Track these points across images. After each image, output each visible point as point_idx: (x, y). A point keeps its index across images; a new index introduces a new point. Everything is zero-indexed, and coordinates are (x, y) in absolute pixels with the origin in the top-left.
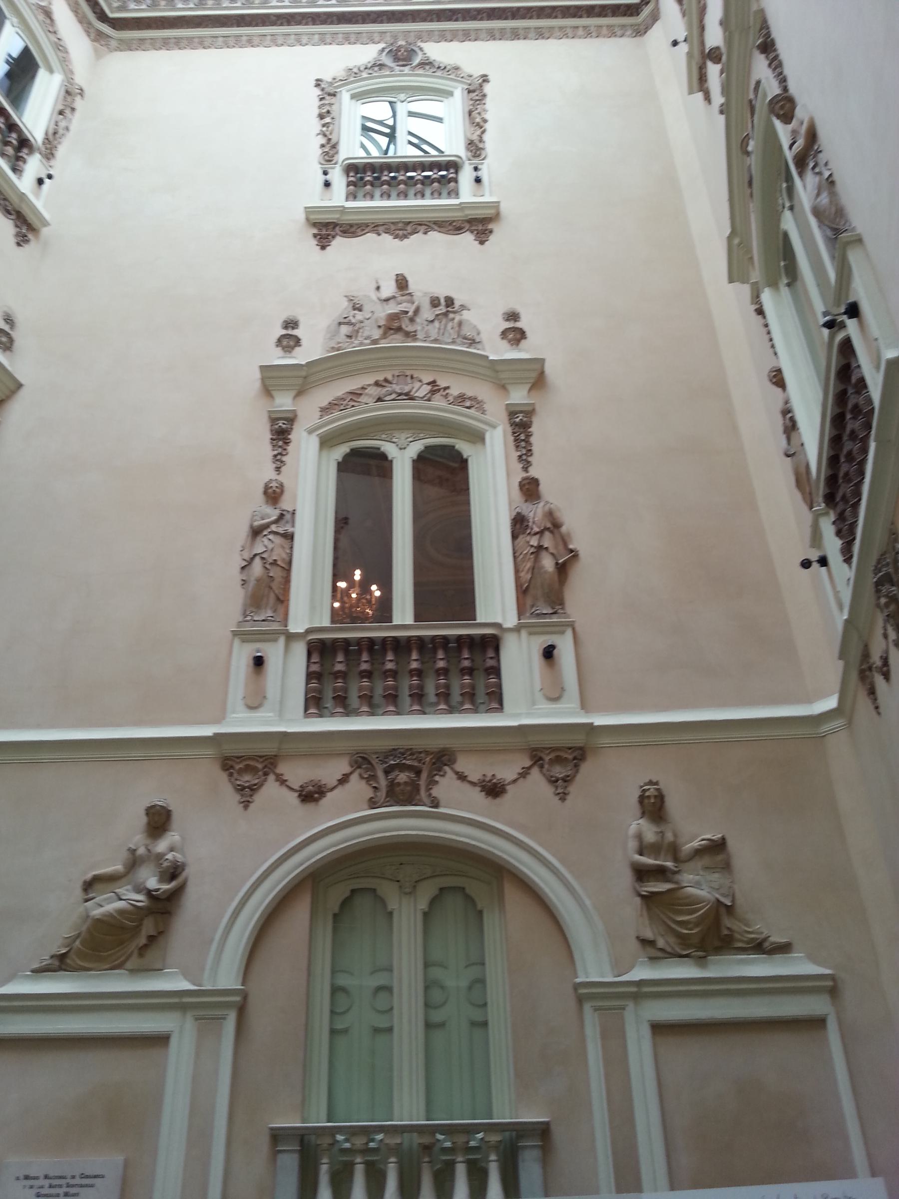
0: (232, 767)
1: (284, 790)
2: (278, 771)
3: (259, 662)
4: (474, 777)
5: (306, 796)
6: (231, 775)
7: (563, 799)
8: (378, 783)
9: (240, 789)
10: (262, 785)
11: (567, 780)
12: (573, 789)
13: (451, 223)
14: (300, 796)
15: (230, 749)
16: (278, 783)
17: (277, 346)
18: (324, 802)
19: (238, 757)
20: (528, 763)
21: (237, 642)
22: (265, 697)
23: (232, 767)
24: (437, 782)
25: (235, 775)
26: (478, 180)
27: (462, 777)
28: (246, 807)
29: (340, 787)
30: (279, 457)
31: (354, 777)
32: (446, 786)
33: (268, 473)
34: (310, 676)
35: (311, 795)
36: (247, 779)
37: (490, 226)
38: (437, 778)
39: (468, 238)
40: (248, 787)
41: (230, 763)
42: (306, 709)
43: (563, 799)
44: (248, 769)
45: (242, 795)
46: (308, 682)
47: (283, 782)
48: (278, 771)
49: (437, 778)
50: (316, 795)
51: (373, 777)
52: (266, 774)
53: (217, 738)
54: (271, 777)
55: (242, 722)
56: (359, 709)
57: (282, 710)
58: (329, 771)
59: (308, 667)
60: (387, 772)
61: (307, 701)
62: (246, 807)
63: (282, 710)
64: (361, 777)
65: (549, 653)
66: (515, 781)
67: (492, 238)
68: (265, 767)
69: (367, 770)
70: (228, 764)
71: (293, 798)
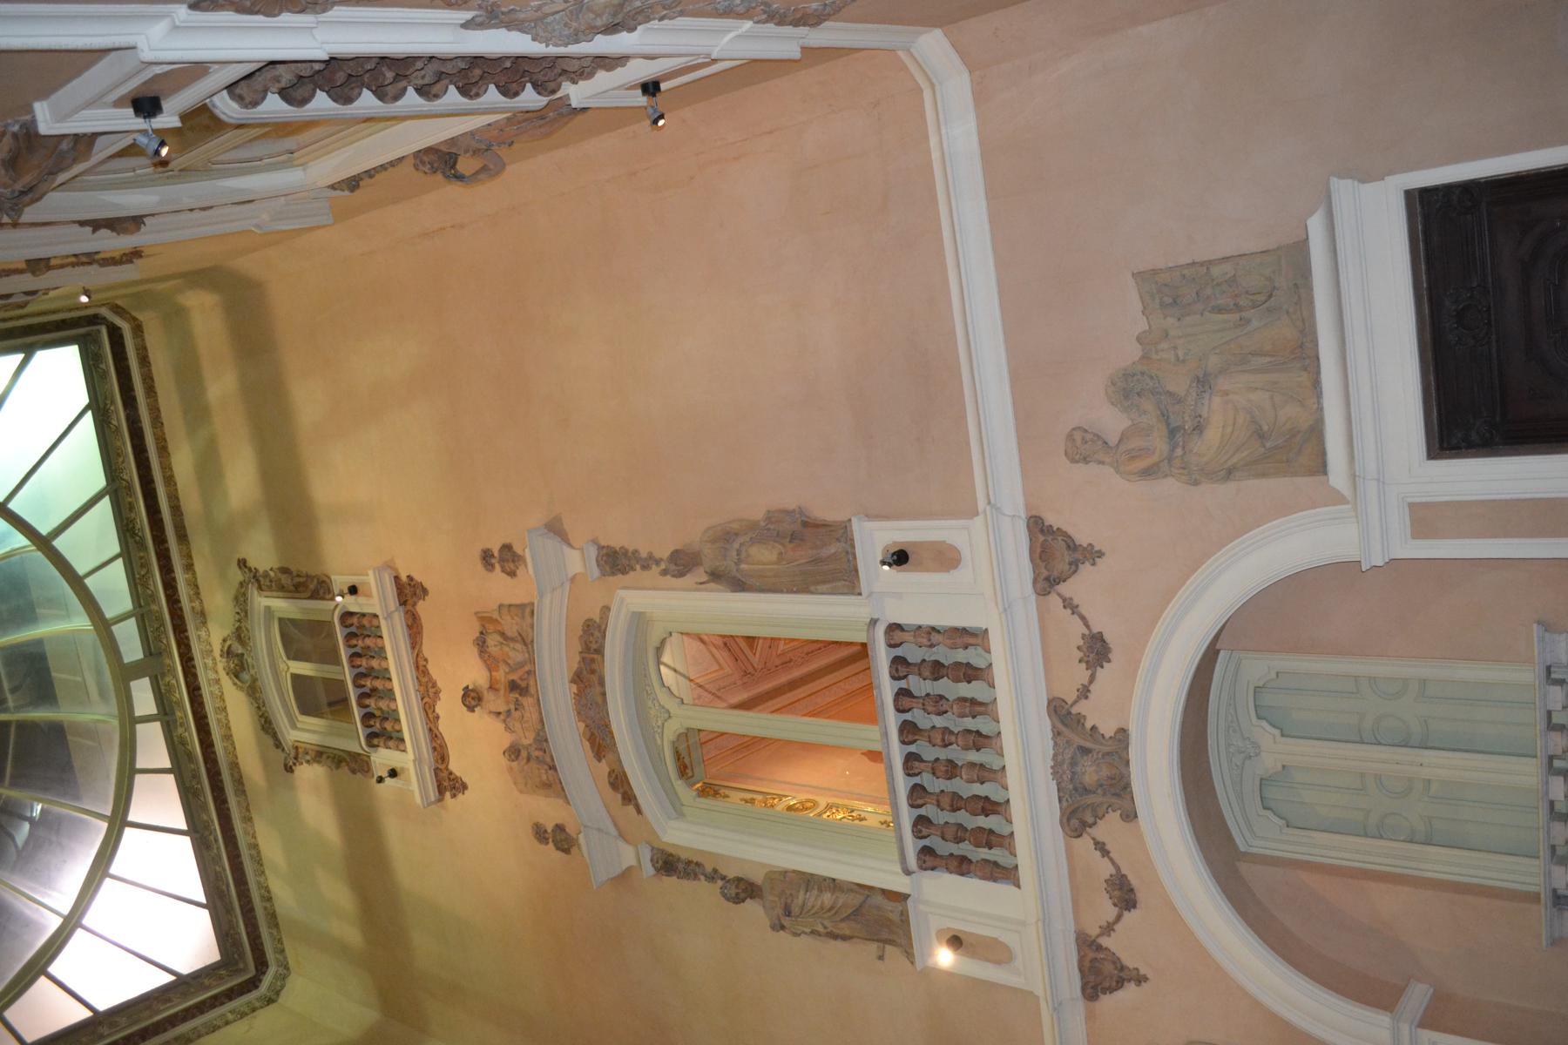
2: (1098, 931)
4: (1082, 674)
7: (1100, 554)
9: (1120, 983)
11: (1072, 546)
12: (1082, 539)
13: (410, 627)
18: (1134, 881)
20: (1054, 601)
24: (1094, 728)
26: (353, 590)
27: (1084, 692)
32: (1099, 714)
37: (404, 578)
38: (1088, 725)
39: (422, 608)
43: (1100, 554)
47: (1109, 929)
48: (1094, 931)
49: (1088, 725)
52: (1099, 948)
54: (1105, 942)
65: (900, 558)
66: (1083, 618)
67: (418, 577)
71: (1128, 916)
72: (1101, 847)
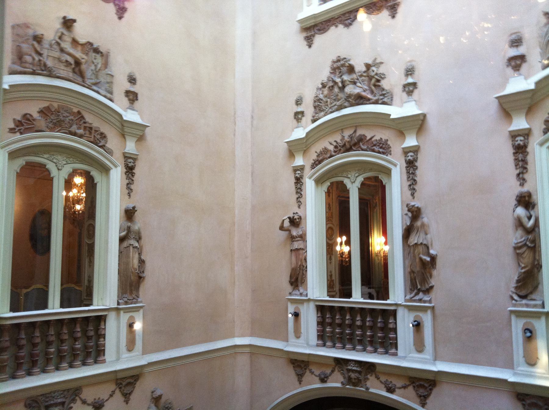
6: (524, 405)
17: (508, 66)
21: (513, 318)
23: (523, 400)
30: (521, 176)
33: (516, 189)
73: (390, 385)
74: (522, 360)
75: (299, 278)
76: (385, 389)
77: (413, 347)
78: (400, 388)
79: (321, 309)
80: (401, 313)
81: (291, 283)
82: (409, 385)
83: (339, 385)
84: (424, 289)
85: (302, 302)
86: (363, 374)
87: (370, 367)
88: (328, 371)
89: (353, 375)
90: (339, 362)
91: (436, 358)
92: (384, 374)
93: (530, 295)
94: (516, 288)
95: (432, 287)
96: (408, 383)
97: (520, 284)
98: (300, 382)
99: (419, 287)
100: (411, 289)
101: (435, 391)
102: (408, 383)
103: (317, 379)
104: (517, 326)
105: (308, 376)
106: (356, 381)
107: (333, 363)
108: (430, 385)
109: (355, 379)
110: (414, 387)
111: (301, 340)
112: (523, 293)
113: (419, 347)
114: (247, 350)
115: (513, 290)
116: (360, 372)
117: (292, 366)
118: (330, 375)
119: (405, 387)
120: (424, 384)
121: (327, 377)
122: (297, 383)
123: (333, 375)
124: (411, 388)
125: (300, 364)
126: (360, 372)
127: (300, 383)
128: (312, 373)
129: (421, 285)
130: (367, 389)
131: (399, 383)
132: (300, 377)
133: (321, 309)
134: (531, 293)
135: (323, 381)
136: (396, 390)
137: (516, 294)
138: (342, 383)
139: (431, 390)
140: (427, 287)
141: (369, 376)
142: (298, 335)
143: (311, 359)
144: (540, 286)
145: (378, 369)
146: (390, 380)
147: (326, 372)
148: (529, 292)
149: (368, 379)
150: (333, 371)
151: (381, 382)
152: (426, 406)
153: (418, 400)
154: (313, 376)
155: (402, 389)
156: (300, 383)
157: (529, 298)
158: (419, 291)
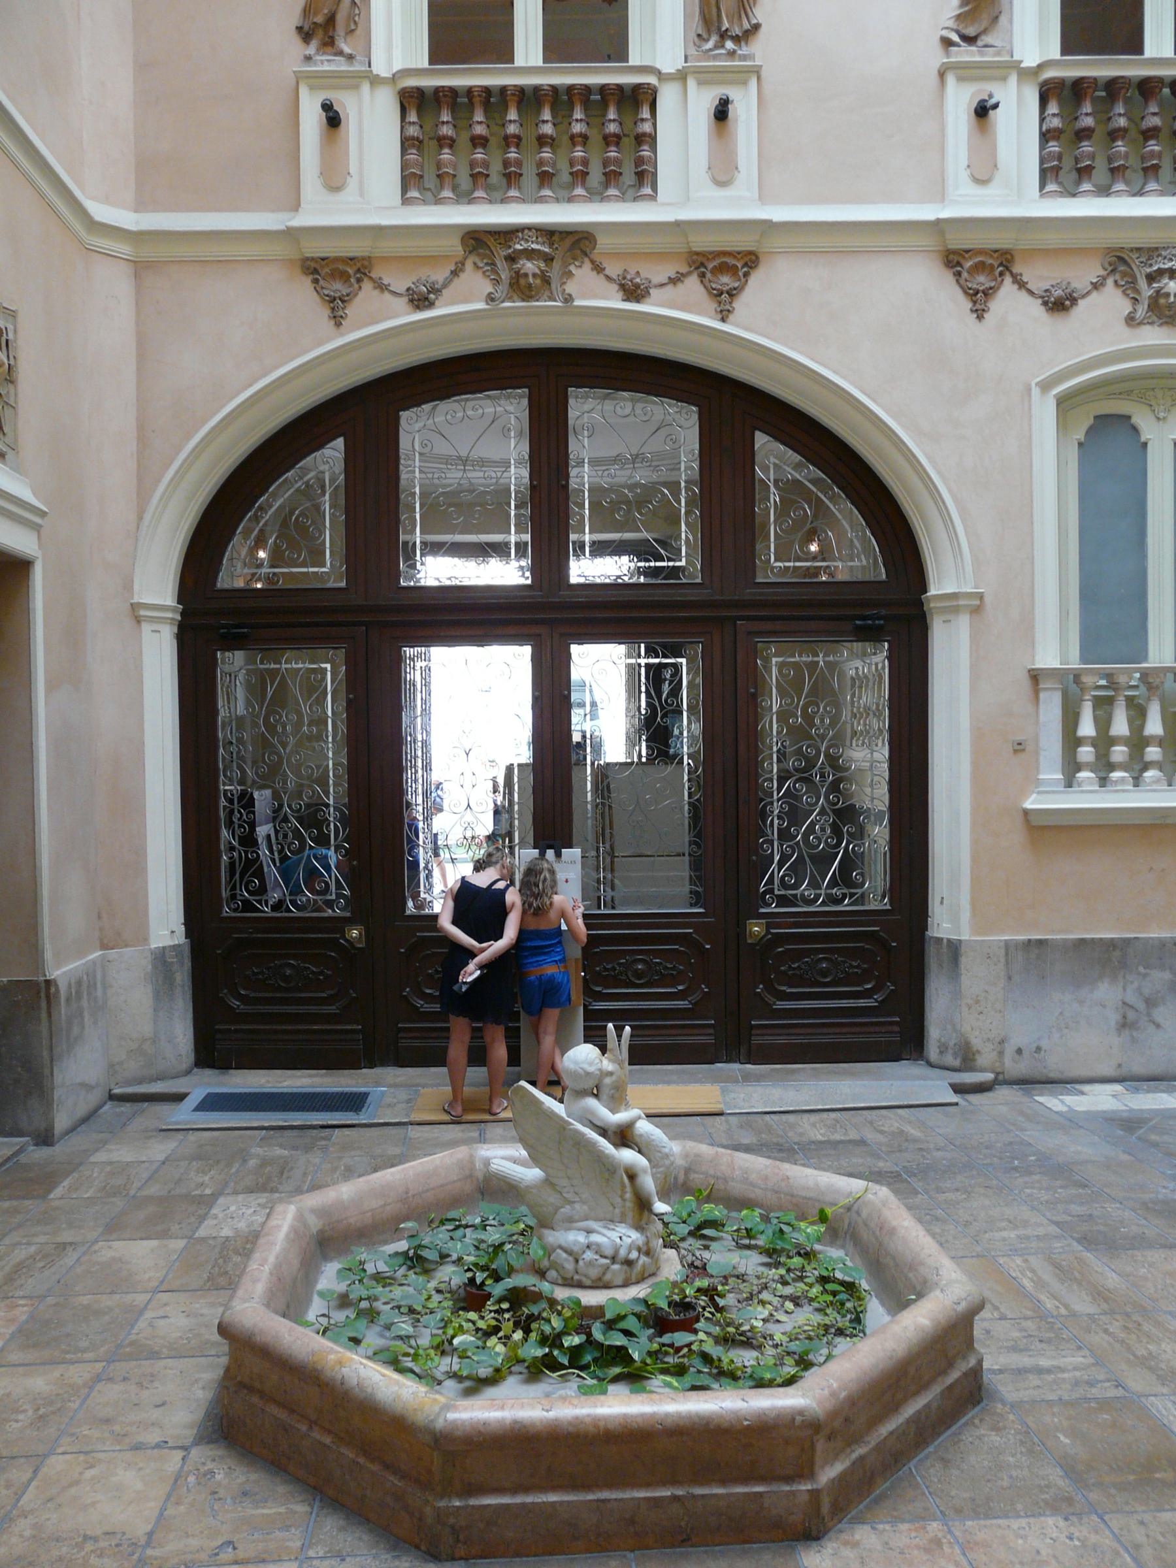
0: (959, 264)
1: (1024, 293)
2: (1015, 270)
3: (983, 111)
5: (1054, 303)
6: (958, 274)
8: (1137, 291)
10: (998, 288)
14: (1045, 303)
15: (958, 241)
16: (1016, 287)
19: (967, 251)
22: (996, 166)
23: (959, 264)
25: (965, 275)
28: (980, 318)
29: (1095, 294)
31: (1110, 282)
34: (1046, 136)
35: (1060, 304)
36: (983, 281)
40: (983, 292)
41: (956, 258)
42: (1042, 185)
44: (980, 267)
45: (975, 302)
46: (1042, 147)
47: (1022, 285)
50: (1067, 303)
51: (1133, 282)
52: (1001, 274)
53: (938, 221)
54: (1008, 280)
55: (968, 203)
56: (1110, 187)
57: (1011, 188)
58: (1082, 274)
59: (1042, 120)
60: (1151, 278)
61: (1043, 173)
62: (980, 318)
63: (1011, 188)
64: (1116, 282)
68: (1001, 264)
69: (1124, 274)
70: (953, 260)
71: (1036, 308)
72: (1096, 286)
73: (638, 280)
74: (964, 175)
75: (340, 18)
76: (621, 294)
77: (705, 178)
78: (662, 285)
79: (415, 101)
80: (667, 98)
81: (305, 34)
82: (689, 273)
83: (481, 306)
84: (737, 31)
85: (352, 81)
86: (556, 265)
87: (576, 242)
88: (439, 275)
89: (529, 266)
90: (478, 240)
91: (763, 198)
92: (618, 255)
93: (983, 37)
94: (958, 17)
95: (757, 27)
96: (684, 269)
97: (966, 9)
98: (337, 320)
99: (726, 25)
100: (699, 36)
101: (755, 279)
102: (684, 269)
103: (402, 303)
104: (960, 100)
105: (366, 298)
106: (538, 281)
107: (459, 250)
108: (746, 265)
109: (534, 275)
110: (702, 276)
111: (350, 193)
112: (971, 31)
113: (723, 173)
114: (123, 249)
115: (951, 23)
116: (548, 259)
117: (307, 281)
118: (445, 286)
119: (673, 281)
120: (724, 264)
121: (436, 290)
122: (327, 325)
123: (456, 281)
124: (693, 282)
125: (336, 272)
126: (548, 259)
127: (338, 325)
128: (381, 287)
129: (731, 22)
130: (568, 299)
131: (658, 273)
132: (336, 308)
133: (415, 101)
134: (985, 31)
135: (420, 301)
136: (651, 291)
137: (957, 32)
138: (490, 298)
139: (746, 275)
140: (746, 26)
141: (572, 268)
142: (334, 179)
143: (387, 247)
144: (1003, 19)
145: (604, 242)
146: (632, 272)
147: (433, 278)
148: (982, 28)
149: (570, 274)
150: (455, 273)
151: (608, 278)
152: (731, 317)
153: (712, 306)
154: (387, 295)
155: (670, 287)
156: (338, 325)
157: (980, 43)
158: (723, 36)
